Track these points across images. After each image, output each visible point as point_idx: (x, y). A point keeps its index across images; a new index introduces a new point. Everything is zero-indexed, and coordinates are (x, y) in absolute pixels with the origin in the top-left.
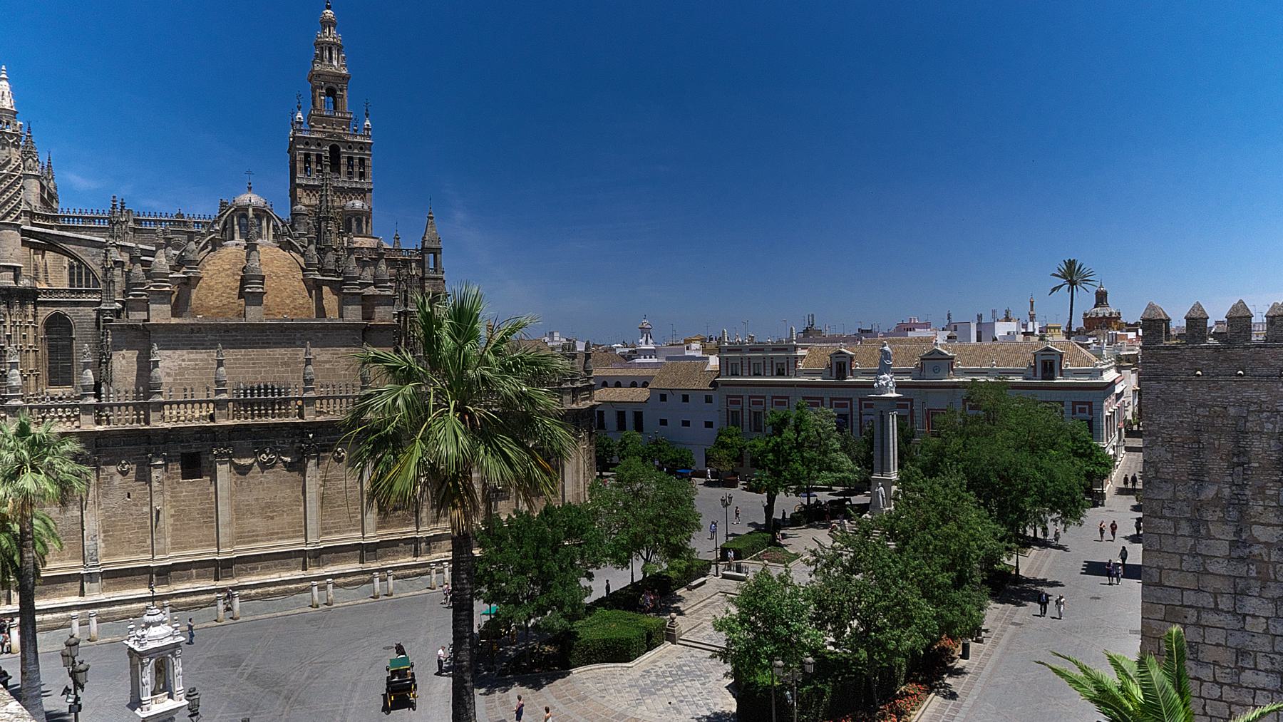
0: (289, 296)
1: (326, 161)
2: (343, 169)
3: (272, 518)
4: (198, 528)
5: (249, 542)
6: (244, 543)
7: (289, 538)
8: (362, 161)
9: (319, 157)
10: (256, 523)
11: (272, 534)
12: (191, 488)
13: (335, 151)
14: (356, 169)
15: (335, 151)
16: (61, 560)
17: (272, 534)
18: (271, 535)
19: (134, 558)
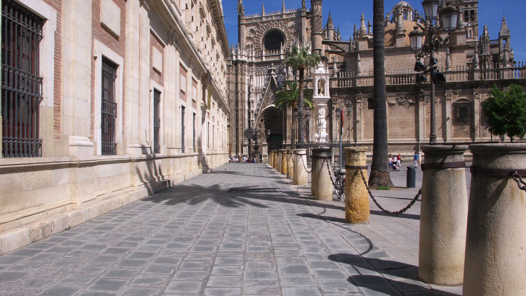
3: (404, 128)
5: (394, 138)
6: (392, 138)
8: (472, 12)
11: (404, 135)
14: (469, 17)
17: (404, 135)
18: (403, 136)
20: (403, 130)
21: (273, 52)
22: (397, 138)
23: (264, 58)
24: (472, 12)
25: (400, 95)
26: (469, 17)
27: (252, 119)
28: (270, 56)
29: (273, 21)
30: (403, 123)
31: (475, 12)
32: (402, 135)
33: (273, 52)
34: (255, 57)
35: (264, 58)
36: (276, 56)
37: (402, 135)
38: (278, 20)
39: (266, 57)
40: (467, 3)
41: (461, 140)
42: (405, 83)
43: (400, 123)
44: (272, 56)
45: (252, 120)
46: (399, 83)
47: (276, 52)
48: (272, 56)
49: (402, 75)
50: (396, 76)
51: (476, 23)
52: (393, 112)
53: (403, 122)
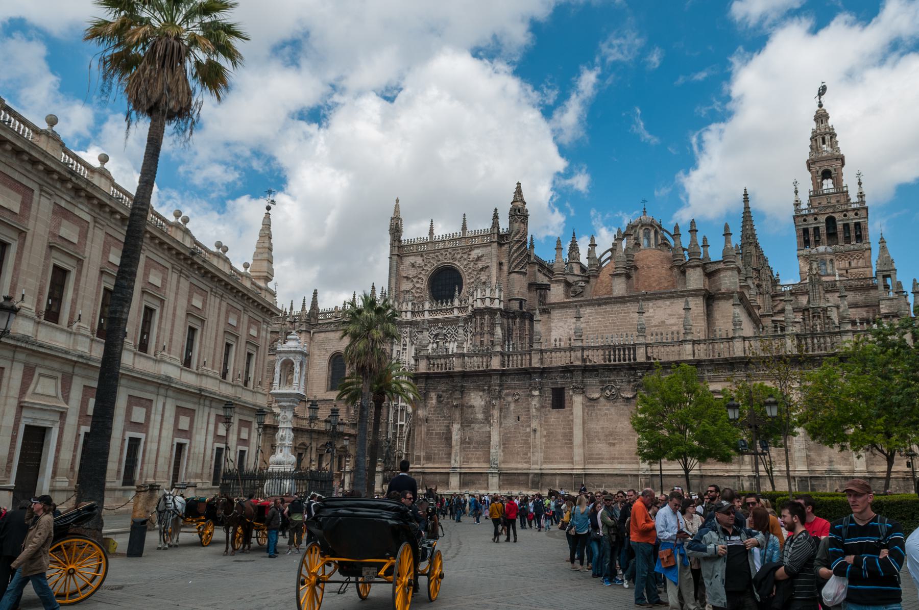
0: (655, 281)
1: (823, 227)
2: (841, 236)
3: (614, 445)
4: (561, 447)
5: (596, 463)
6: (593, 463)
7: (626, 463)
9: (816, 229)
10: (601, 447)
11: (614, 458)
12: (554, 416)
13: (831, 221)
14: (853, 234)
15: (831, 221)
16: (478, 462)
17: (614, 458)
18: (612, 459)
19: (520, 466)
20: (612, 448)
21: (442, 303)
22: (602, 463)
23: (426, 313)
24: (857, 225)
25: (605, 382)
26: (853, 234)
27: (399, 423)
28: (436, 311)
29: (446, 249)
30: (611, 435)
31: (862, 226)
32: (610, 459)
33: (442, 303)
34: (412, 312)
35: (426, 313)
36: (447, 310)
37: (610, 459)
38: (454, 249)
39: (430, 312)
40: (847, 211)
41: (715, 470)
42: (615, 361)
43: (606, 436)
44: (441, 310)
45: (402, 426)
46: (620, 360)
47: (447, 303)
48: (441, 310)
49: (624, 345)
50: (614, 348)
51: (866, 246)
52: (594, 415)
53: (611, 434)
